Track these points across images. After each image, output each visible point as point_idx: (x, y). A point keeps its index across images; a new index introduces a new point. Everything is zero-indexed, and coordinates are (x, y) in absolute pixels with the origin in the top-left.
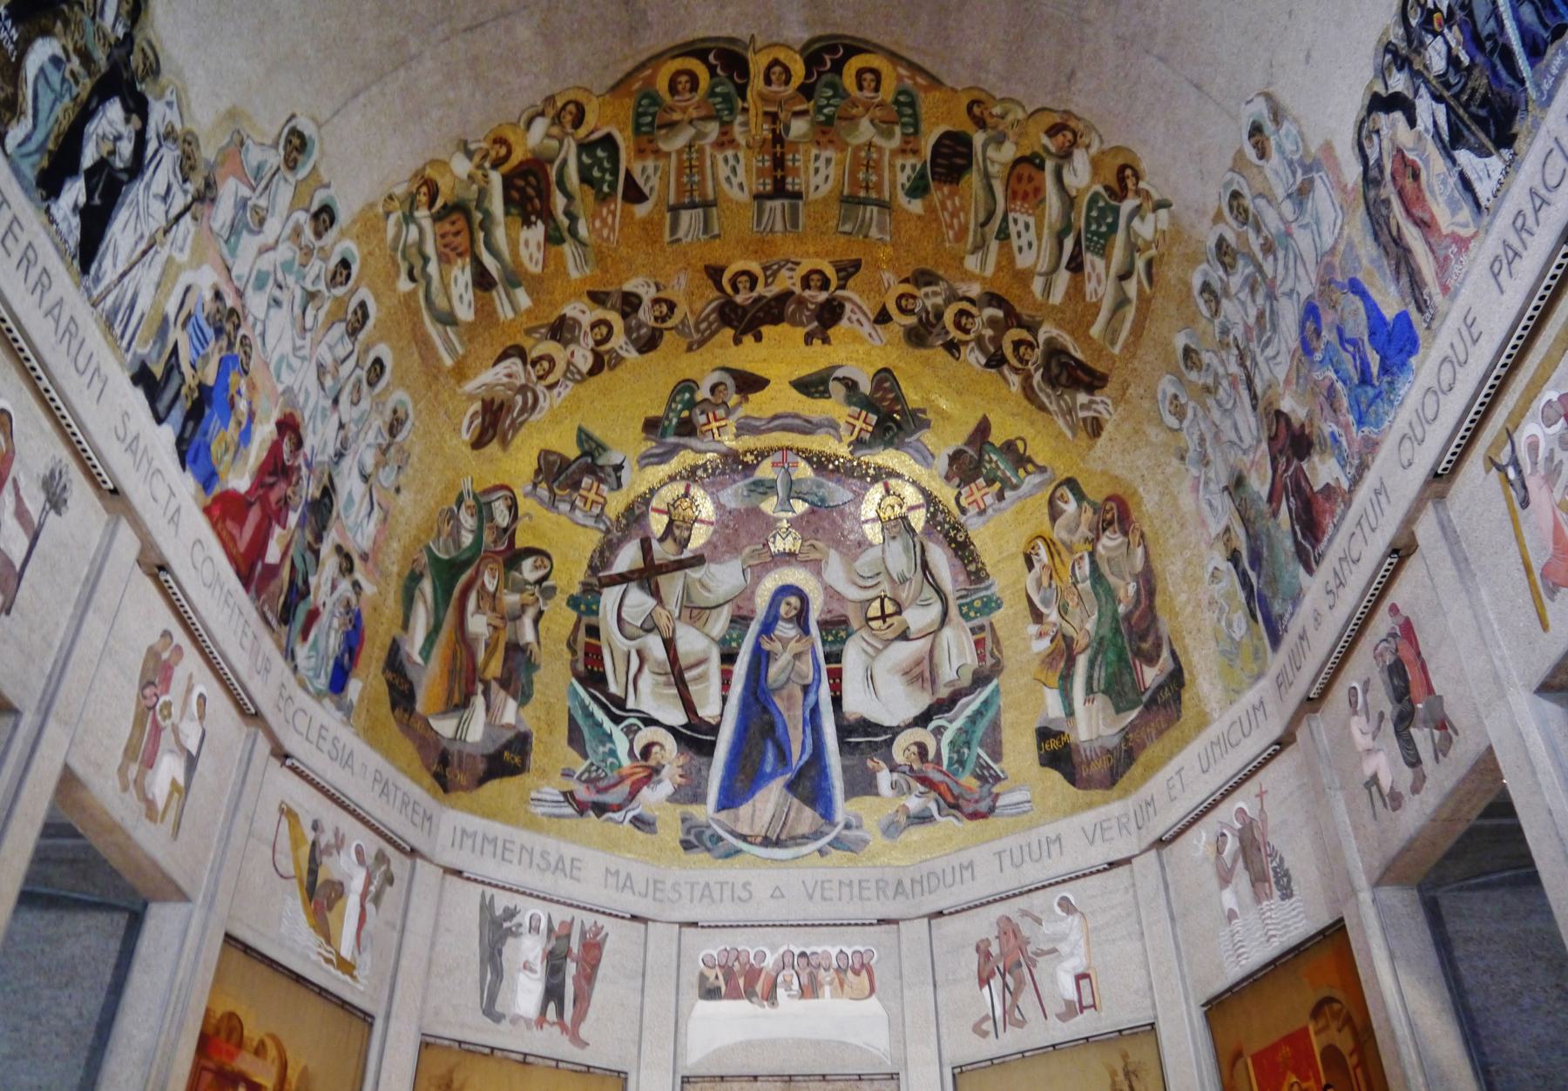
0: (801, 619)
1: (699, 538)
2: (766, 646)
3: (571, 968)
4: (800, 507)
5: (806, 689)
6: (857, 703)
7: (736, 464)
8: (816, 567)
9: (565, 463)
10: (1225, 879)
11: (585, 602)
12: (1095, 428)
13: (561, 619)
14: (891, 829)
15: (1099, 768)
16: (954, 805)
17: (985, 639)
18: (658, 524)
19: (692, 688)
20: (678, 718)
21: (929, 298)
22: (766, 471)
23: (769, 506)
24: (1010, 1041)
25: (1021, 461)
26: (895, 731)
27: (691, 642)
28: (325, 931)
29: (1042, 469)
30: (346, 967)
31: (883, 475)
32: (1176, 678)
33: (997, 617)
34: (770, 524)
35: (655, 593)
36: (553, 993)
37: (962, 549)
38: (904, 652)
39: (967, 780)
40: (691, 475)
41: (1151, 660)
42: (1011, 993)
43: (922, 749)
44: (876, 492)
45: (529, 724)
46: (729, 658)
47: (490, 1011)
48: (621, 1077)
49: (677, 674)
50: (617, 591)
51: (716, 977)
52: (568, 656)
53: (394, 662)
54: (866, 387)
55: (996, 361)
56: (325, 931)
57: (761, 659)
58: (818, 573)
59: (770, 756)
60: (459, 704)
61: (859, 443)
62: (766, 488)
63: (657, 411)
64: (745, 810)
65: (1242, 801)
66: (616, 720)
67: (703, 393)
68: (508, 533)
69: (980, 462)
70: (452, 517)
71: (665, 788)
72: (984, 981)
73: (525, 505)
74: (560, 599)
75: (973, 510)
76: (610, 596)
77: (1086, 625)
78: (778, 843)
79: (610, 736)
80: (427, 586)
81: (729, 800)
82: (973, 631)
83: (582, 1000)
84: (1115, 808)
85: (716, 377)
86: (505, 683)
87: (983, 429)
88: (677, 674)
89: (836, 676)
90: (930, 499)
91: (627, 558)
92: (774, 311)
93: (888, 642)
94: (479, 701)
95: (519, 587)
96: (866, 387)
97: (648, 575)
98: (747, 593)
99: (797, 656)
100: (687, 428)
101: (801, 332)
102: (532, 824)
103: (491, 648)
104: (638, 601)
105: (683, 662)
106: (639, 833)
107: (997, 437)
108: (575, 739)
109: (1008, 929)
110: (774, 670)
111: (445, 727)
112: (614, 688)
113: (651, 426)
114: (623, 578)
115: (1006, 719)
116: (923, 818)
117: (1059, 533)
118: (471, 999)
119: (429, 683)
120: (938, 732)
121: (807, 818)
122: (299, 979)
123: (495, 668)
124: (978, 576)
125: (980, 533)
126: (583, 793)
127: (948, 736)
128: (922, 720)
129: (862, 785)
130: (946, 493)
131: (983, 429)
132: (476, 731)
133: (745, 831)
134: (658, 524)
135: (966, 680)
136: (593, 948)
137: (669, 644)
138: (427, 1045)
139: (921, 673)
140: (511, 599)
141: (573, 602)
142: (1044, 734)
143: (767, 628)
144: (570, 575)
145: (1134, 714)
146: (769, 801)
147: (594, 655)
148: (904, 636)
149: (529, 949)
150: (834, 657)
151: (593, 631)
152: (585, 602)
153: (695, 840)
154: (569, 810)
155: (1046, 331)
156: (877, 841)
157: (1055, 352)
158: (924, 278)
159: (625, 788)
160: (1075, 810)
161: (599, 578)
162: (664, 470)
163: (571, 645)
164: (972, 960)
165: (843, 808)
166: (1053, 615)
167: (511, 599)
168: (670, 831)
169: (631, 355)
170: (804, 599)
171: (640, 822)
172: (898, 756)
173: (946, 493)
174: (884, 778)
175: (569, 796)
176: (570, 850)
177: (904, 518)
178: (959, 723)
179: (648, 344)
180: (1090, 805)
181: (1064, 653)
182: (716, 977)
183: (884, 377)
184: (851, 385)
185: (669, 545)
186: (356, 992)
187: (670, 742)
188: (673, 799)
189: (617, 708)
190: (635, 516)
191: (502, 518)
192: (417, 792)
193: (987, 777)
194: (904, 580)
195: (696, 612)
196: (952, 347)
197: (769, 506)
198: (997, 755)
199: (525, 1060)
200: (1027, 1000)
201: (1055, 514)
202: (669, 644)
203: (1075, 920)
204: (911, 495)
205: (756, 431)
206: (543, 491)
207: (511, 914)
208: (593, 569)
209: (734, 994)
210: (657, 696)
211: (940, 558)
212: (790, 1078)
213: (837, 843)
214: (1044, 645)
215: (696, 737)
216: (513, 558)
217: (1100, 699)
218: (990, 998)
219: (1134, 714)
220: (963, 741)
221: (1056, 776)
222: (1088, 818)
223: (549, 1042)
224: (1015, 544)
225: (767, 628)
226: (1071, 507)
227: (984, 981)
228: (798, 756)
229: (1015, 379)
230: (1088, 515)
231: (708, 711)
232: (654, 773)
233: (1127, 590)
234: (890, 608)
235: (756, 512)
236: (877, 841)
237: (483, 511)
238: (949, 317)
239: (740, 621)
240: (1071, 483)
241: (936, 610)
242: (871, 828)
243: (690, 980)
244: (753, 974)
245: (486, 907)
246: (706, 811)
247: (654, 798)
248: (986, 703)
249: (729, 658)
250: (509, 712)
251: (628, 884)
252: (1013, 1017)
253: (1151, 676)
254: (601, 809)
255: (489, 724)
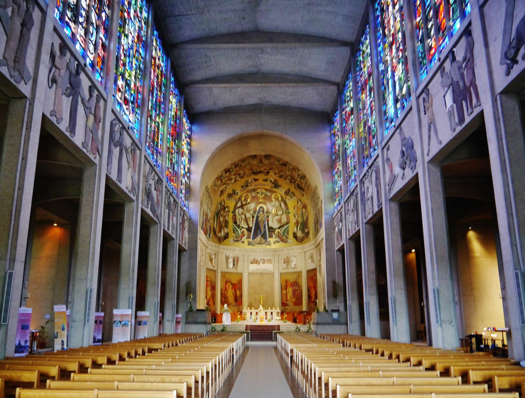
0: (263, 211)
1: (249, 200)
2: (258, 215)
3: (236, 262)
4: (263, 196)
5: (264, 222)
6: (271, 224)
7: (254, 190)
8: (265, 204)
9: (230, 194)
10: (310, 259)
11: (234, 212)
12: (303, 195)
13: (231, 215)
14: (274, 243)
15: (300, 240)
16: (282, 240)
17: (288, 218)
18: (243, 199)
19: (249, 222)
20: (246, 227)
21: (282, 174)
22: (258, 191)
23: (259, 195)
24: (286, 271)
25: (294, 195)
26: (275, 229)
27: (248, 215)
28: (212, 264)
29: (296, 197)
30: (214, 266)
31: (275, 192)
32: (308, 232)
33: (290, 215)
34: (259, 198)
35: (243, 209)
36: (234, 265)
37: (286, 204)
38: (277, 217)
39: (284, 238)
40: (248, 192)
41: (307, 229)
42: (287, 266)
43: (279, 232)
44: (274, 194)
45: (228, 231)
46: (253, 217)
47: (227, 267)
48: (242, 274)
49: (246, 220)
50: (238, 209)
51: (252, 261)
52: (232, 220)
53: (214, 230)
54: (273, 181)
55: (291, 182)
56: (212, 264)
57: (258, 217)
58: (266, 205)
59: (259, 232)
60: (220, 231)
61: (272, 188)
62: (258, 193)
63: (243, 184)
64: (256, 240)
65: (312, 251)
66: (239, 228)
67: (250, 181)
68: (224, 205)
69: (288, 193)
70: (217, 207)
71: (245, 237)
72: (284, 263)
73: (226, 201)
74: (231, 212)
75: (287, 199)
76: (237, 210)
77: (300, 220)
78: (260, 244)
79: (238, 231)
80: (216, 217)
81: (254, 238)
82: (287, 216)
83: (237, 265)
84: (300, 246)
85: (251, 180)
86: (225, 226)
87: (289, 190)
88: (246, 220)
89: (268, 220)
90: (282, 197)
91: (239, 204)
92: (260, 172)
93: (275, 216)
94: (223, 230)
95: (225, 212)
96: (273, 181)
97: (242, 207)
98: (256, 208)
99: (263, 217)
100: (247, 186)
101: (263, 175)
102: (230, 245)
103: (223, 222)
104: (241, 210)
105: (247, 218)
106: (242, 244)
107: (291, 190)
108: (234, 232)
109: (287, 258)
110: (259, 219)
111: (219, 235)
112: (238, 223)
113: (242, 187)
114: (239, 207)
115: (290, 230)
116: (278, 242)
117: (298, 206)
118: (225, 266)
119: (217, 230)
120: (281, 230)
121: (264, 241)
122: (210, 270)
123: (224, 225)
124: (287, 208)
125: (287, 201)
126: (235, 239)
127: (282, 231)
128: (279, 228)
129: (271, 236)
130: (284, 196)
131: (289, 190)
132: (223, 234)
133: (256, 242)
134: (243, 199)
135: (285, 223)
136: (238, 259)
137: (245, 216)
138: (221, 272)
139: (279, 221)
140: (225, 214)
141: (232, 212)
142: (294, 234)
143: (258, 213)
144: (231, 209)
145: (304, 235)
146: (259, 238)
147: (235, 219)
148: (277, 215)
149: (231, 260)
150: (268, 217)
151: (235, 216)
152: (234, 212)
153: (249, 244)
154: (234, 242)
155: (297, 182)
156: (272, 244)
157: (298, 185)
158: (281, 171)
159: (240, 238)
160: (296, 245)
161: (235, 208)
162: (244, 192)
163: (232, 218)
164: (283, 261)
165: (269, 239)
166: (297, 217)
167: (225, 214)
168: (246, 243)
169: (240, 179)
170: (264, 209)
171: (243, 242)
172: (276, 232)
173: (284, 196)
174: (274, 236)
175: (234, 240)
176: (235, 248)
177: (278, 199)
178: (284, 229)
179: (242, 177)
180: (298, 245)
181: (297, 223)
182: (252, 261)
183: (275, 180)
184: (271, 181)
185: (245, 202)
186: (215, 269)
187: (246, 231)
188: (247, 238)
189: (239, 226)
190: (240, 199)
191: (223, 204)
192: (218, 245)
193: (287, 238)
194: (277, 207)
195: (248, 211)
196: (285, 179)
197: (259, 195)
198: (288, 234)
199: (231, 273)
200: (289, 266)
201: (298, 203)
202: (245, 216)
203: (295, 258)
204: (279, 196)
205: (257, 186)
206: (228, 198)
207: (229, 256)
208: (235, 207)
209: (254, 263)
210: (244, 224)
211: (283, 205)
212: (261, 274)
213: (268, 244)
214: (295, 221)
215: (249, 230)
216: (225, 209)
217: (301, 231)
218: (285, 265)
219: (304, 235)
220: (284, 232)
221: (295, 240)
222: (298, 246)
223: (234, 271)
224: (293, 206)
225: (258, 213)
226: (300, 203)
227: (284, 263)
228: (263, 232)
229: (293, 185)
230: (302, 205)
231: (251, 225)
232: (244, 235)
233: (305, 218)
234: (276, 211)
235: (257, 196)
236: (272, 244)
237: (221, 204)
238: (285, 176)
239: (255, 212)
240: (300, 200)
241: (282, 212)
242: (272, 242)
243: (249, 261)
244: (257, 261)
245: (226, 256)
246: (250, 240)
247: (244, 239)
248: (287, 227)
249: (253, 217)
250: (226, 230)
251: (241, 251)
252: (287, 268)
253: (306, 231)
254: (238, 241)
255: (224, 233)
